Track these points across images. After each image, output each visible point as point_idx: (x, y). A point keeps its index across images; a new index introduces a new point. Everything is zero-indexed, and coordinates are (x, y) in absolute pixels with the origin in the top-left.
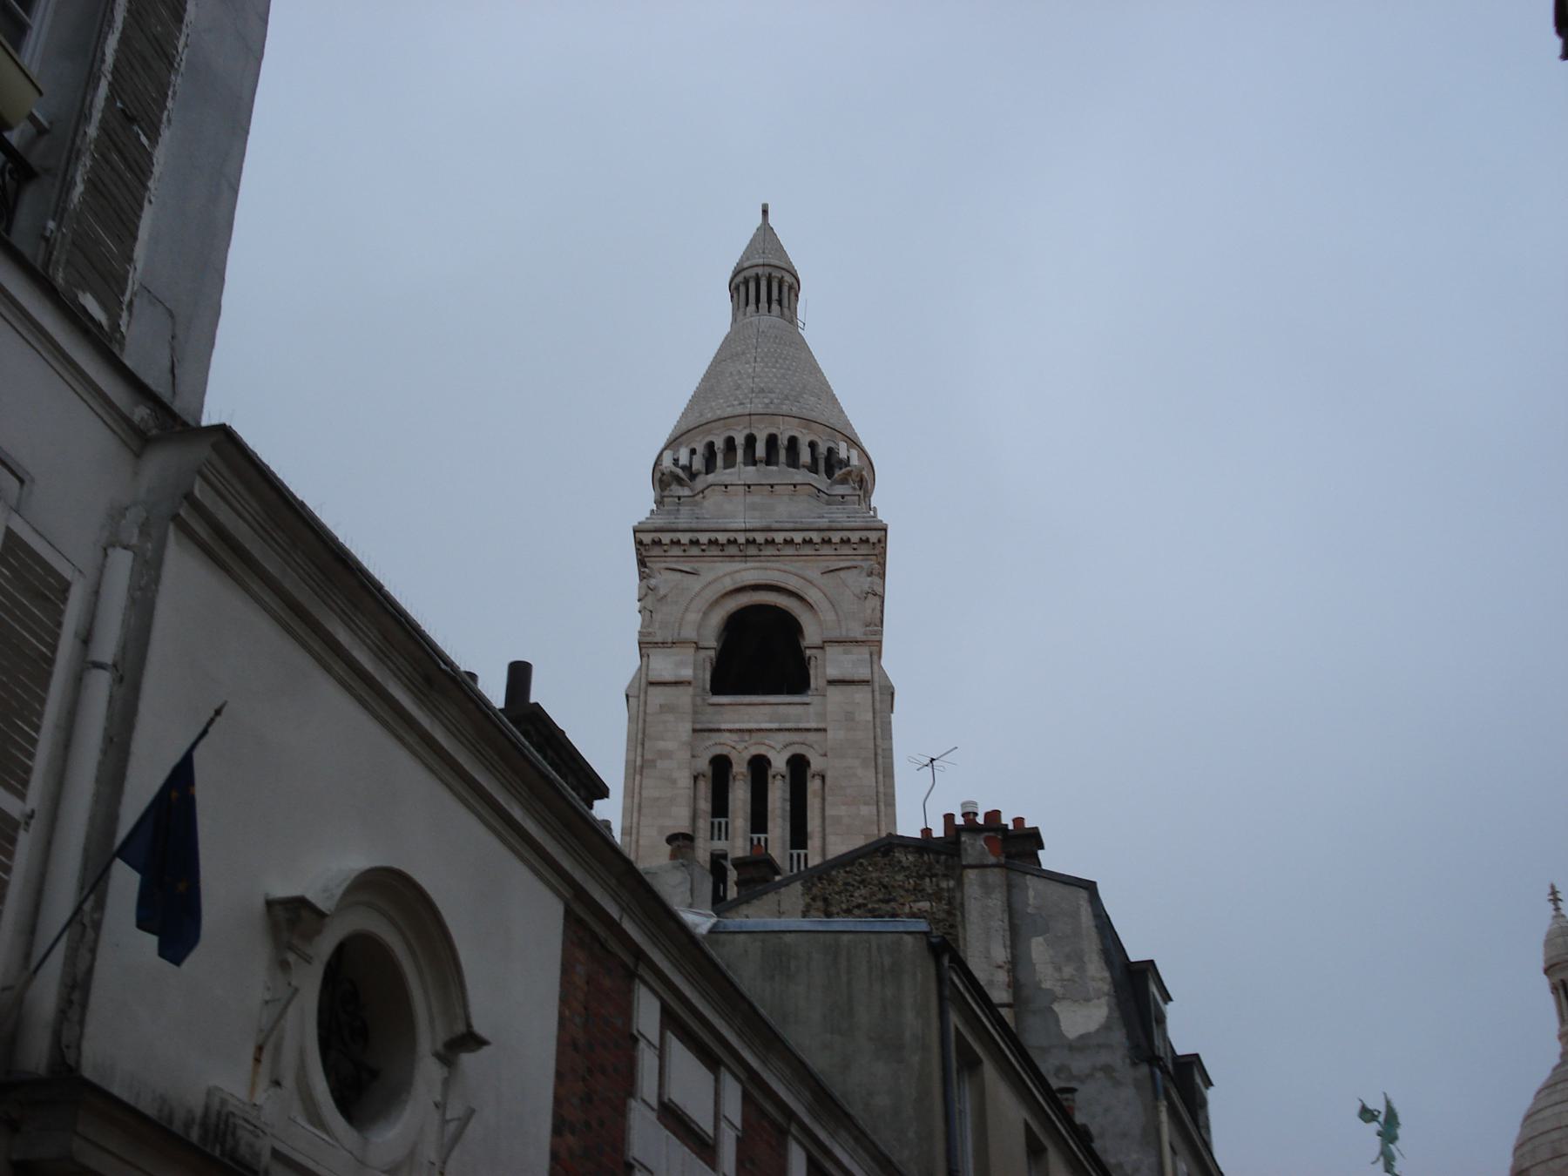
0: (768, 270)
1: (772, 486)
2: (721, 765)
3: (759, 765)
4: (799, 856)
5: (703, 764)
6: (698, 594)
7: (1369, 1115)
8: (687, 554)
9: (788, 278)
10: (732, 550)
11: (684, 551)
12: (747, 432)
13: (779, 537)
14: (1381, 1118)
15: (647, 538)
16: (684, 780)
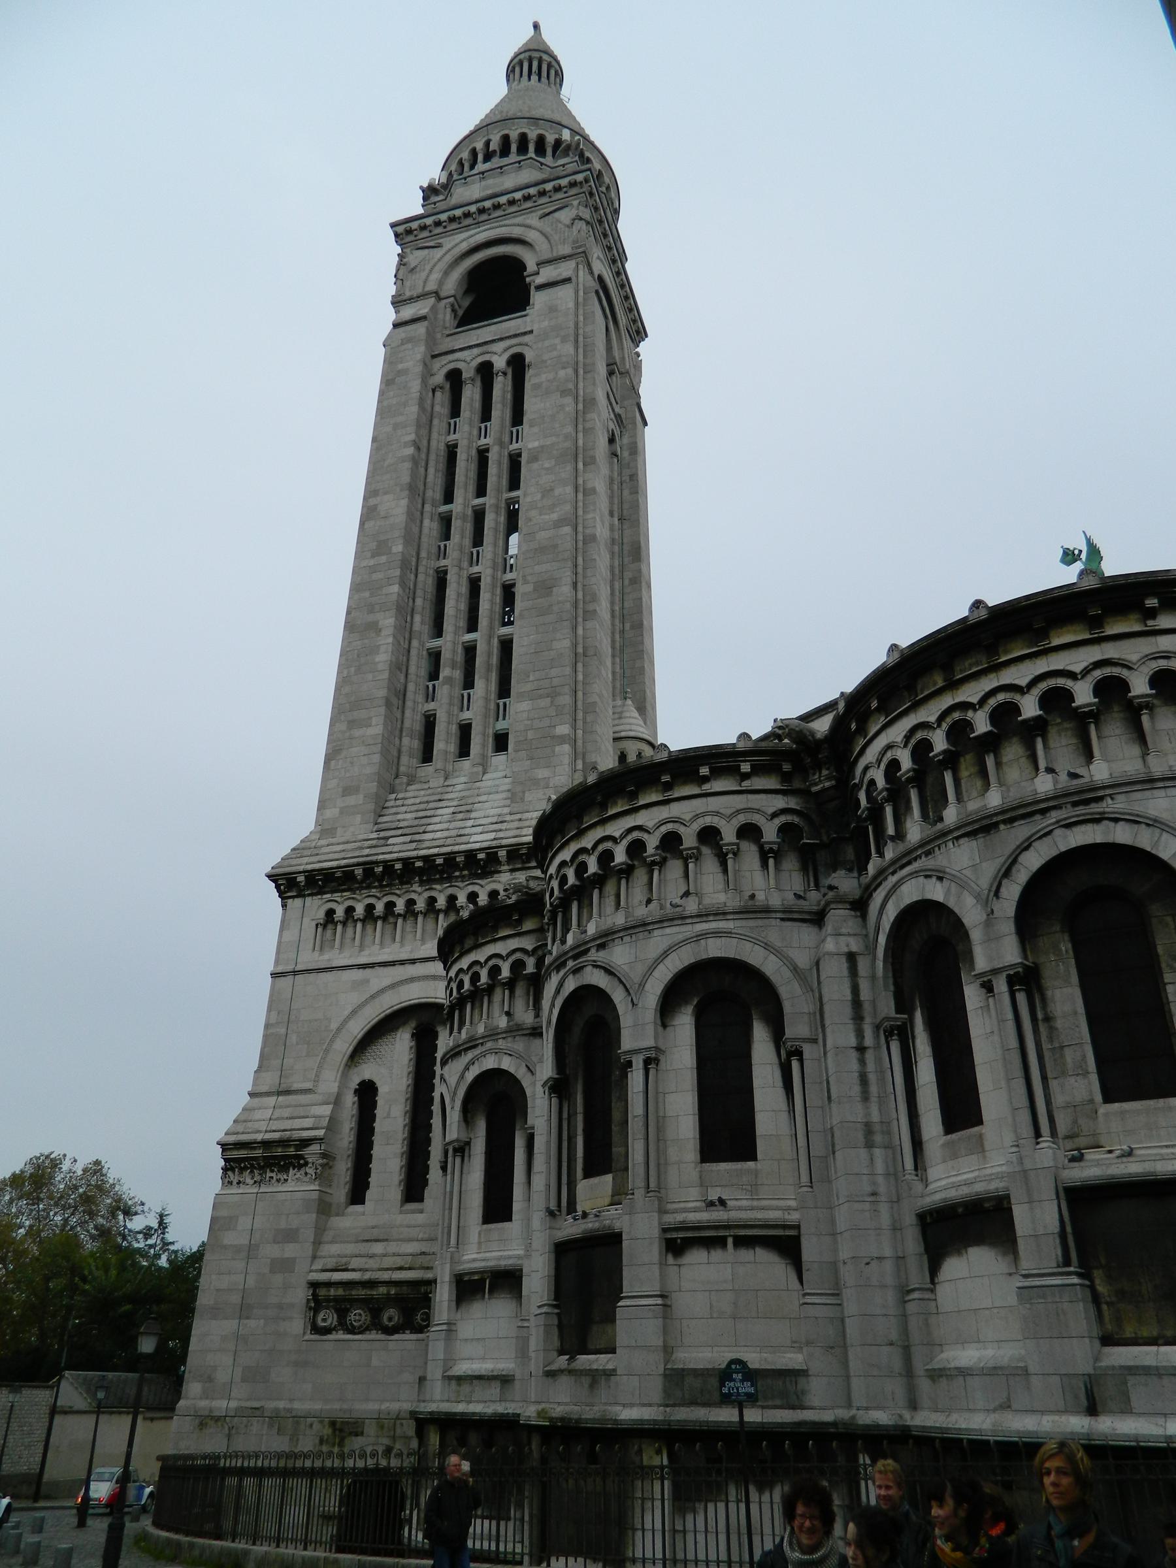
0: (527, 54)
1: (501, 168)
2: (455, 377)
3: (486, 371)
4: (518, 431)
5: (439, 378)
6: (439, 260)
7: (1070, 557)
8: (432, 233)
9: (545, 57)
10: (469, 221)
11: (430, 231)
12: (485, 139)
13: (503, 200)
14: (1084, 556)
15: (400, 229)
16: (415, 386)
